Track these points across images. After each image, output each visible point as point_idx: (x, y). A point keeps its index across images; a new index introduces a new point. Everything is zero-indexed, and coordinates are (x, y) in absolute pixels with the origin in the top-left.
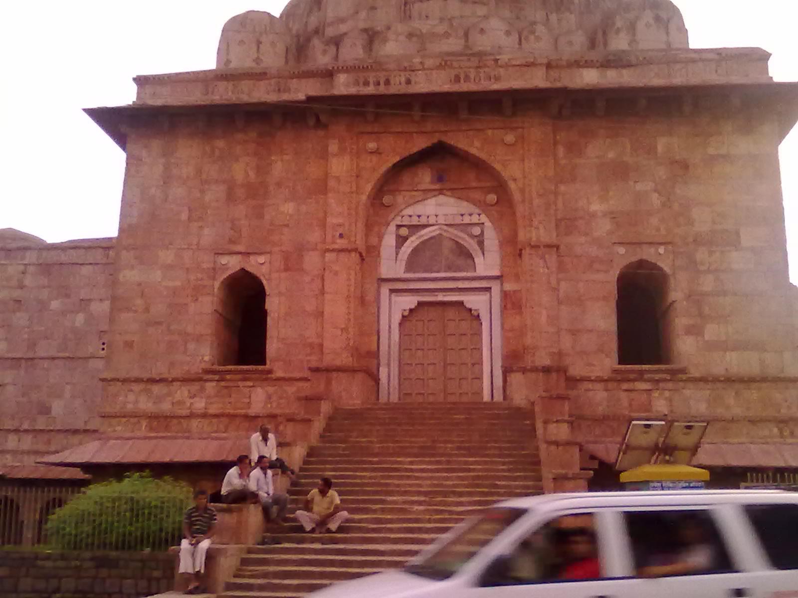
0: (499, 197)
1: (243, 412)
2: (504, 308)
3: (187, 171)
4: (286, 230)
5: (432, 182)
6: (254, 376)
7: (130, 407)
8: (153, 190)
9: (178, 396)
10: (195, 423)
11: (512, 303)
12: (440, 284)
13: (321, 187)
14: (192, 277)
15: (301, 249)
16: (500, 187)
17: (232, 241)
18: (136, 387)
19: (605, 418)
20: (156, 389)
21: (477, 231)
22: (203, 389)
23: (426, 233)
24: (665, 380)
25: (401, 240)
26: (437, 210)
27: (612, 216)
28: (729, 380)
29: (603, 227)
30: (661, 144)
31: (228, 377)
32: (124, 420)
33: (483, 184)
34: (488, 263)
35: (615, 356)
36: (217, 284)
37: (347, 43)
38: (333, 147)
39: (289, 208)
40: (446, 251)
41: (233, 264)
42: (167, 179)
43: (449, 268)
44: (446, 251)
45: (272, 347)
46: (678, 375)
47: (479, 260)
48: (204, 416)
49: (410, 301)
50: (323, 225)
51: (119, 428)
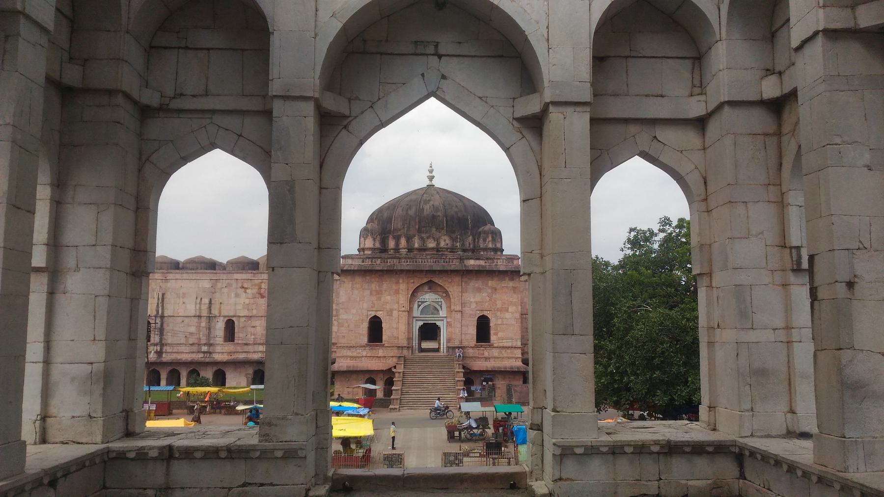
0: (447, 295)
12: (430, 319)
13: (397, 292)
15: (391, 310)
16: (446, 292)
23: (426, 304)
25: (419, 306)
26: (429, 297)
28: (503, 347)
29: (474, 306)
30: (490, 283)
38: (401, 281)
39: (389, 298)
41: (373, 314)
43: (433, 314)
45: (384, 338)
46: (492, 346)
49: (421, 323)
50: (398, 303)
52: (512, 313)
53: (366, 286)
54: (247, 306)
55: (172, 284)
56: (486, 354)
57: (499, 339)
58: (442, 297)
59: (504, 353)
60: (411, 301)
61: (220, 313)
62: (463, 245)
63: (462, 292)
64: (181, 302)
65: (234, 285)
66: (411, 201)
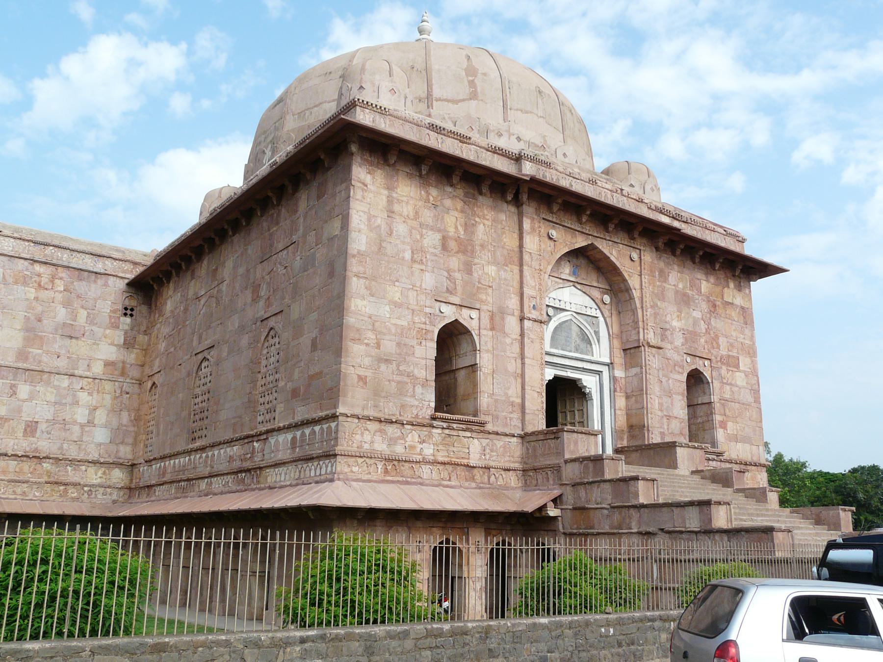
1: (465, 461)
2: (613, 391)
3: (407, 210)
4: (490, 291)
5: (569, 274)
6: (474, 428)
7: (366, 446)
8: (379, 221)
14: (417, 319)
18: (373, 426)
20: (392, 430)
22: (430, 436)
24: (714, 460)
31: (455, 426)
32: (360, 460)
33: (600, 286)
34: (602, 351)
39: (491, 270)
40: (574, 335)
41: (449, 314)
44: (574, 335)
47: (595, 347)
48: (435, 463)
49: (550, 374)
51: (355, 469)
53: (427, 215)
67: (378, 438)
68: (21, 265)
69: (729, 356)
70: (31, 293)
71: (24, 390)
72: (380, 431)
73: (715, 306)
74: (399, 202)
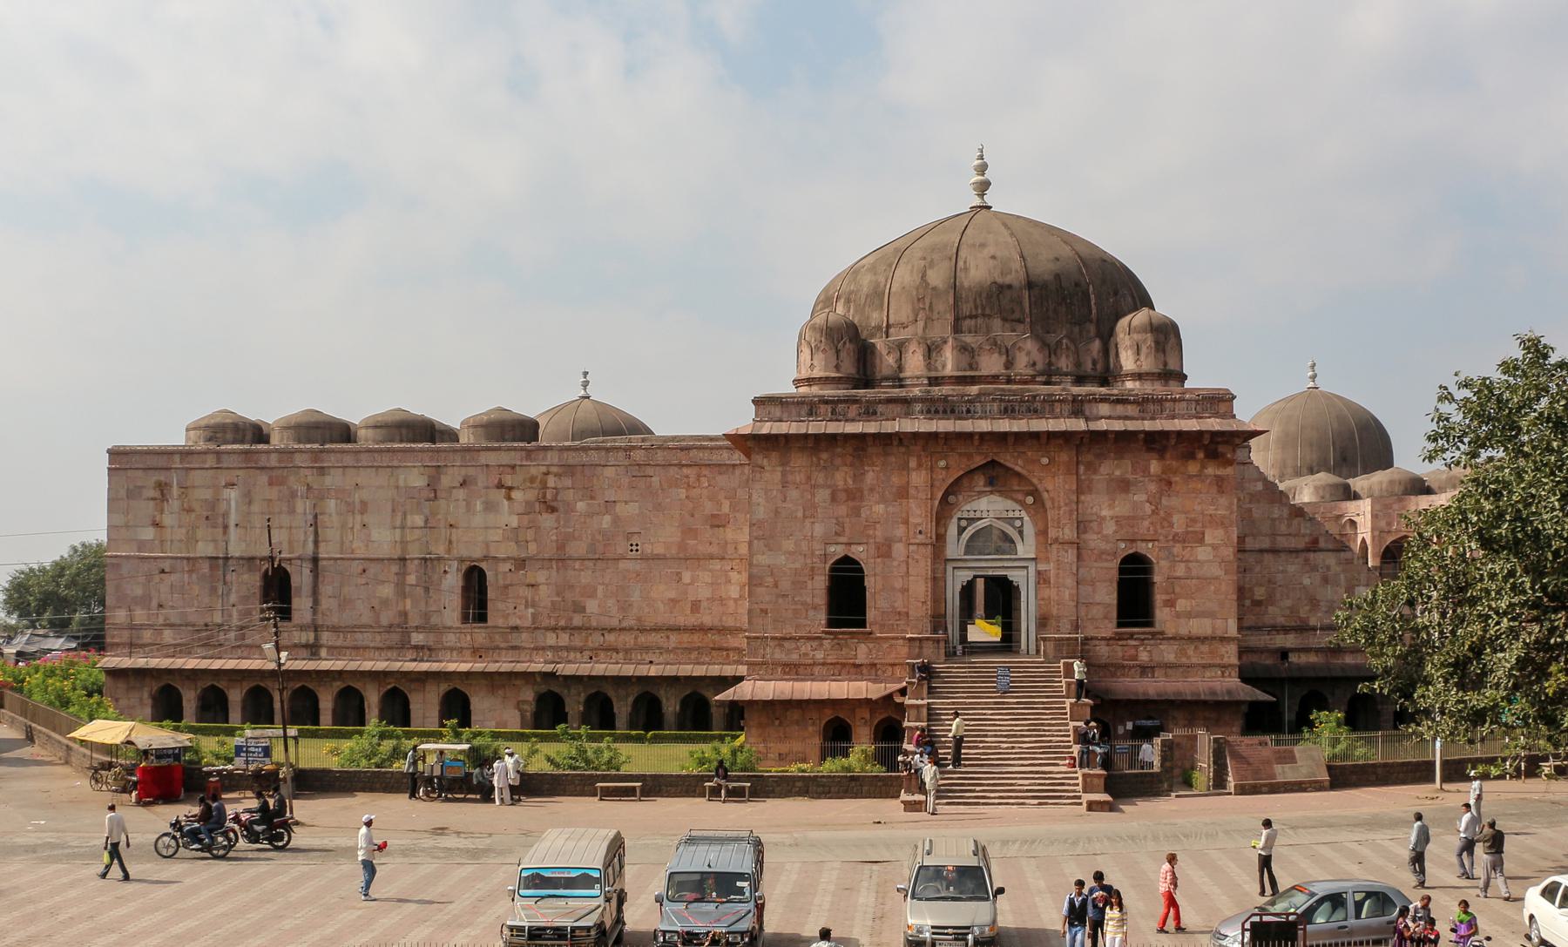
9: (803, 650)
10: (817, 670)
11: (1042, 579)
12: (993, 565)
13: (903, 493)
16: (1034, 492)
17: (836, 534)
19: (1106, 666)
20: (786, 644)
21: (1018, 523)
23: (980, 524)
25: (961, 530)
26: (988, 507)
27: (1118, 520)
28: (1191, 639)
29: (1110, 528)
35: (1115, 621)
36: (828, 566)
37: (913, 347)
38: (913, 463)
39: (880, 509)
40: (995, 538)
41: (838, 551)
42: (785, 484)
43: (997, 552)
44: (995, 538)
45: (871, 615)
47: (1020, 547)
48: (823, 664)
50: (906, 522)
52: (1215, 547)
53: (820, 477)
54: (514, 534)
55: (333, 480)
56: (1144, 657)
57: (1178, 615)
58: (1022, 504)
59: (1193, 656)
60: (942, 515)
61: (449, 551)
62: (1078, 364)
63: (1079, 491)
64: (358, 527)
65: (482, 480)
66: (933, 249)
67: (777, 650)
68: (673, 471)
69: (1187, 533)
70: (682, 493)
71: (687, 577)
72: (781, 646)
73: (1170, 483)
74: (792, 473)
